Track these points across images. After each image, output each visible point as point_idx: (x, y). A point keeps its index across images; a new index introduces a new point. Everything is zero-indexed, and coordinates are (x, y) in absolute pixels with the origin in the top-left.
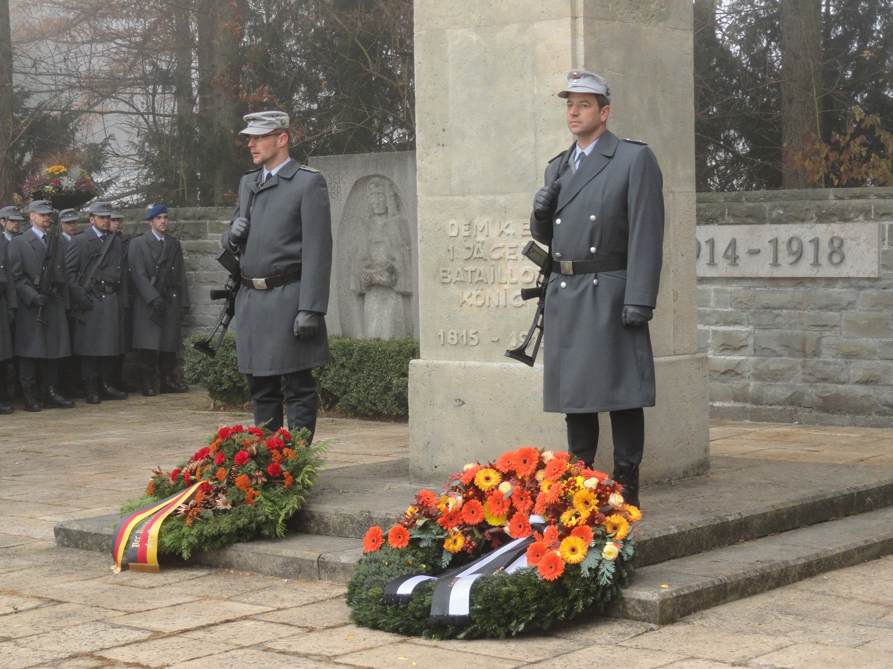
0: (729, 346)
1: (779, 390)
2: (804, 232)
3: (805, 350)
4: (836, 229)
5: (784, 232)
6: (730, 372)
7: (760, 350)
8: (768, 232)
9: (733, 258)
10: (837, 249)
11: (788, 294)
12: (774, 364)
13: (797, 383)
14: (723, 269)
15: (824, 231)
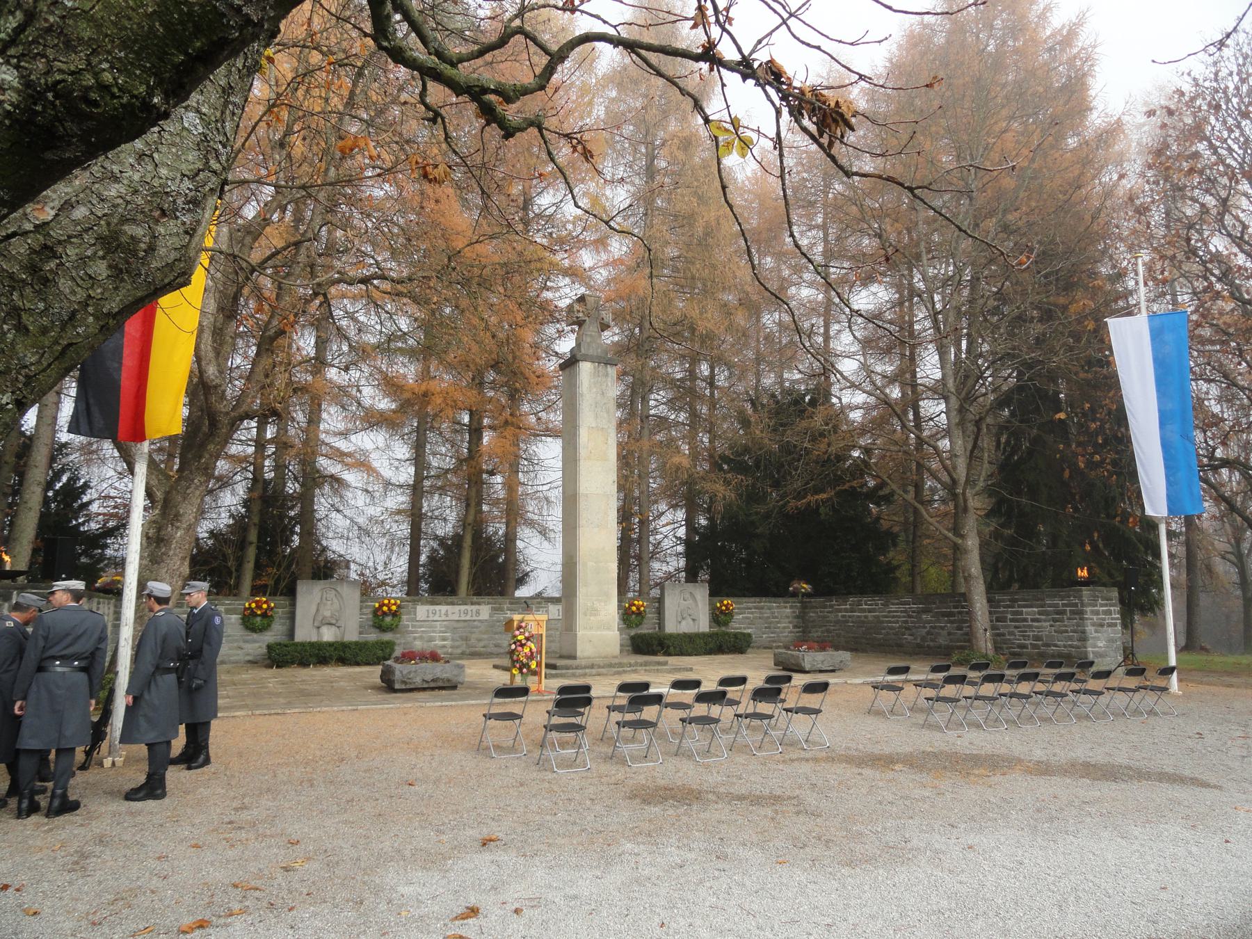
0: (444, 639)
1: (459, 651)
2: (469, 607)
3: (466, 639)
4: (477, 607)
5: (463, 608)
6: (444, 646)
7: (453, 640)
8: (457, 608)
9: (446, 615)
10: (478, 613)
11: (461, 625)
12: (457, 643)
13: (464, 648)
14: (443, 618)
15: (475, 608)
